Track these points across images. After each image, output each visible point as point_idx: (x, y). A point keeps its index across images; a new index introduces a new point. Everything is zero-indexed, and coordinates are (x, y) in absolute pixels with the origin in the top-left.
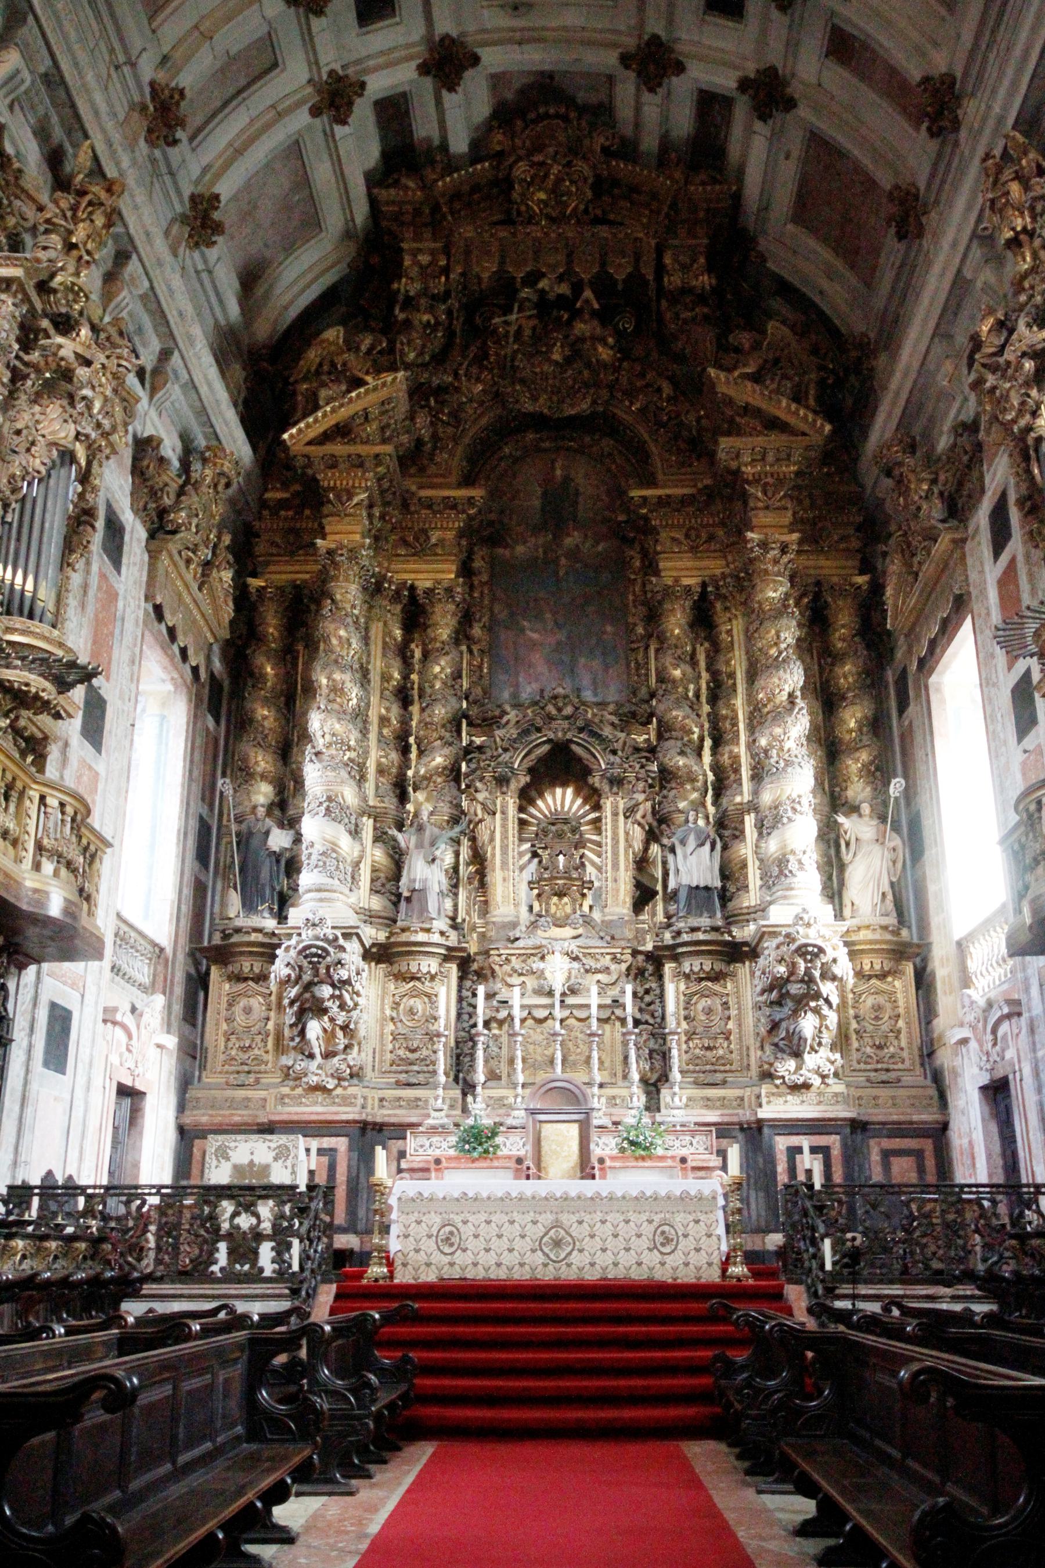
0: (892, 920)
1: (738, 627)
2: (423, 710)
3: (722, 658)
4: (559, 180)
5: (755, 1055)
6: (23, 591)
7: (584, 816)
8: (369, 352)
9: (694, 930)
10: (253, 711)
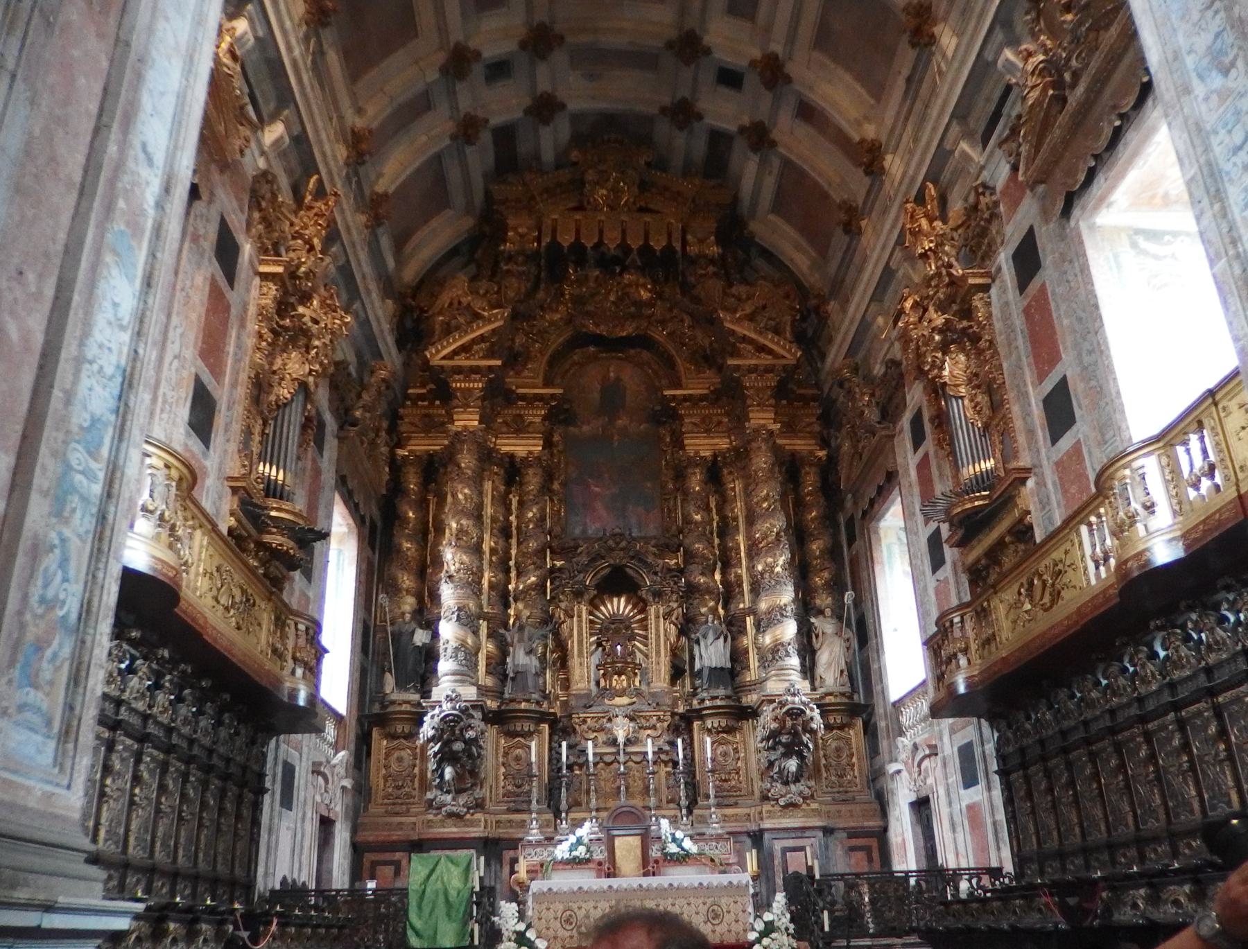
0: (847, 689)
1: (738, 486)
2: (519, 543)
6: (276, 480)
7: (634, 617)
8: (485, 294)
10: (401, 545)
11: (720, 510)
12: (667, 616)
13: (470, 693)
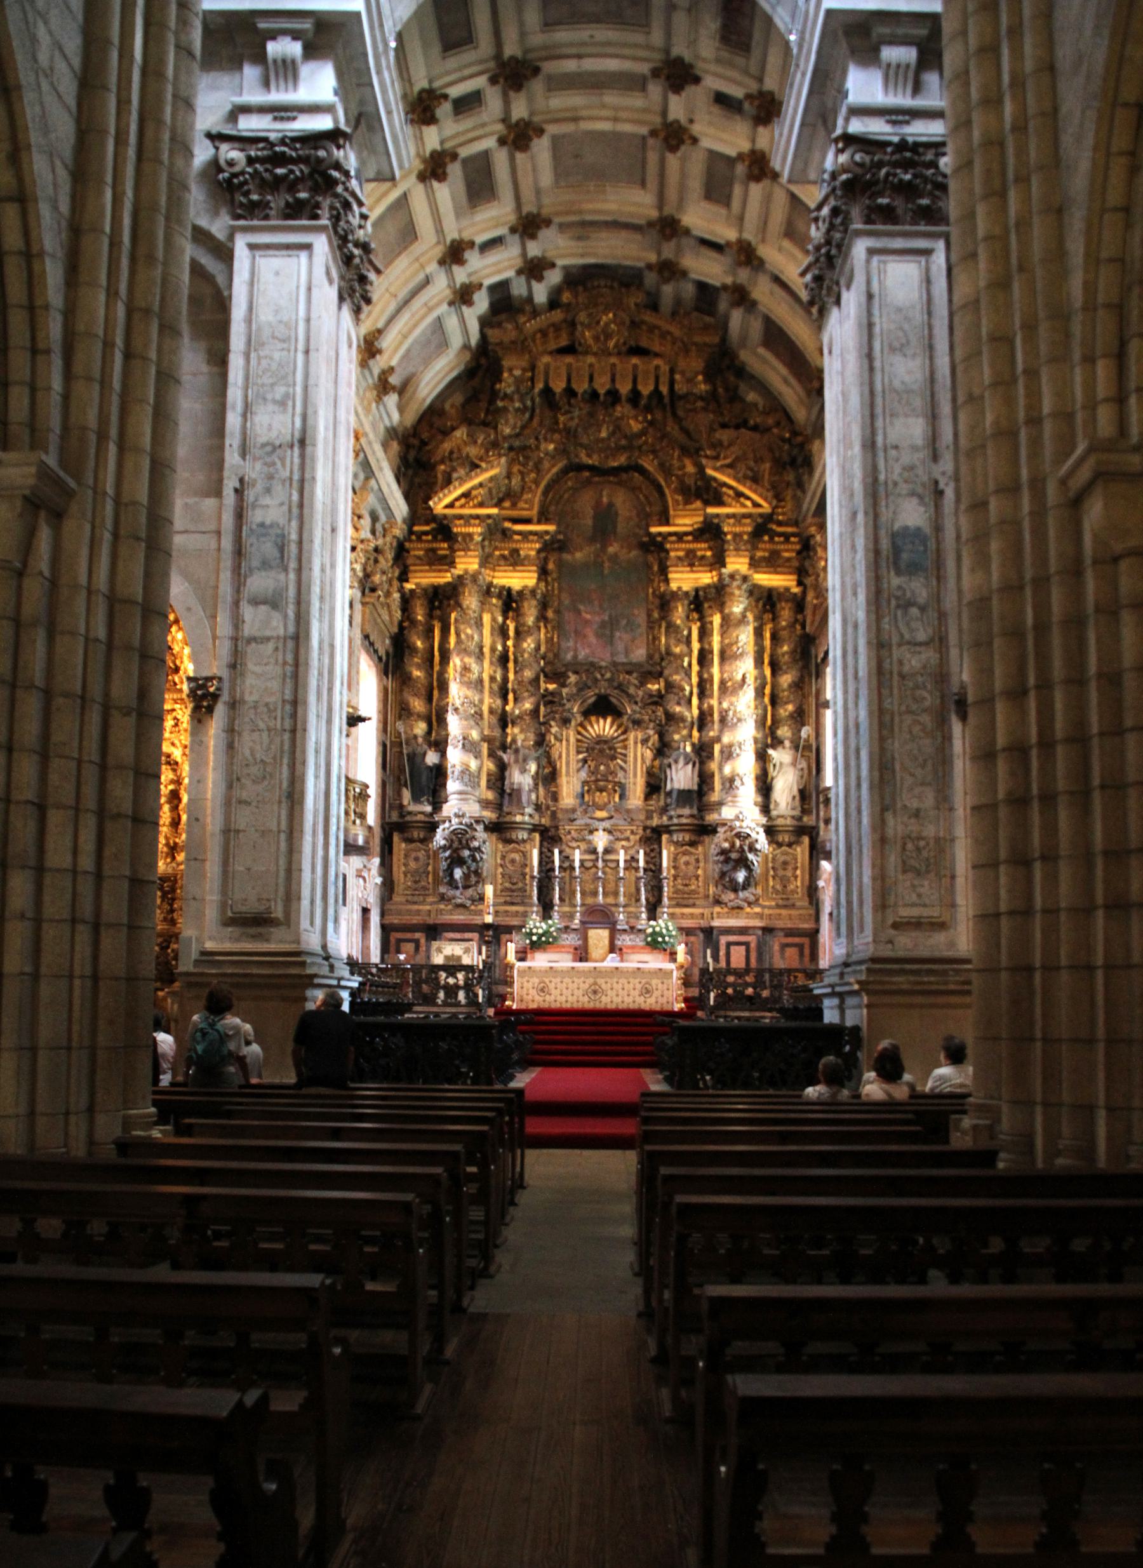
1: (717, 620)
3: (706, 640)
4: (607, 324)
5: (712, 890)
9: (680, 816)
11: (701, 639)
12: (645, 741)
13: (473, 809)
